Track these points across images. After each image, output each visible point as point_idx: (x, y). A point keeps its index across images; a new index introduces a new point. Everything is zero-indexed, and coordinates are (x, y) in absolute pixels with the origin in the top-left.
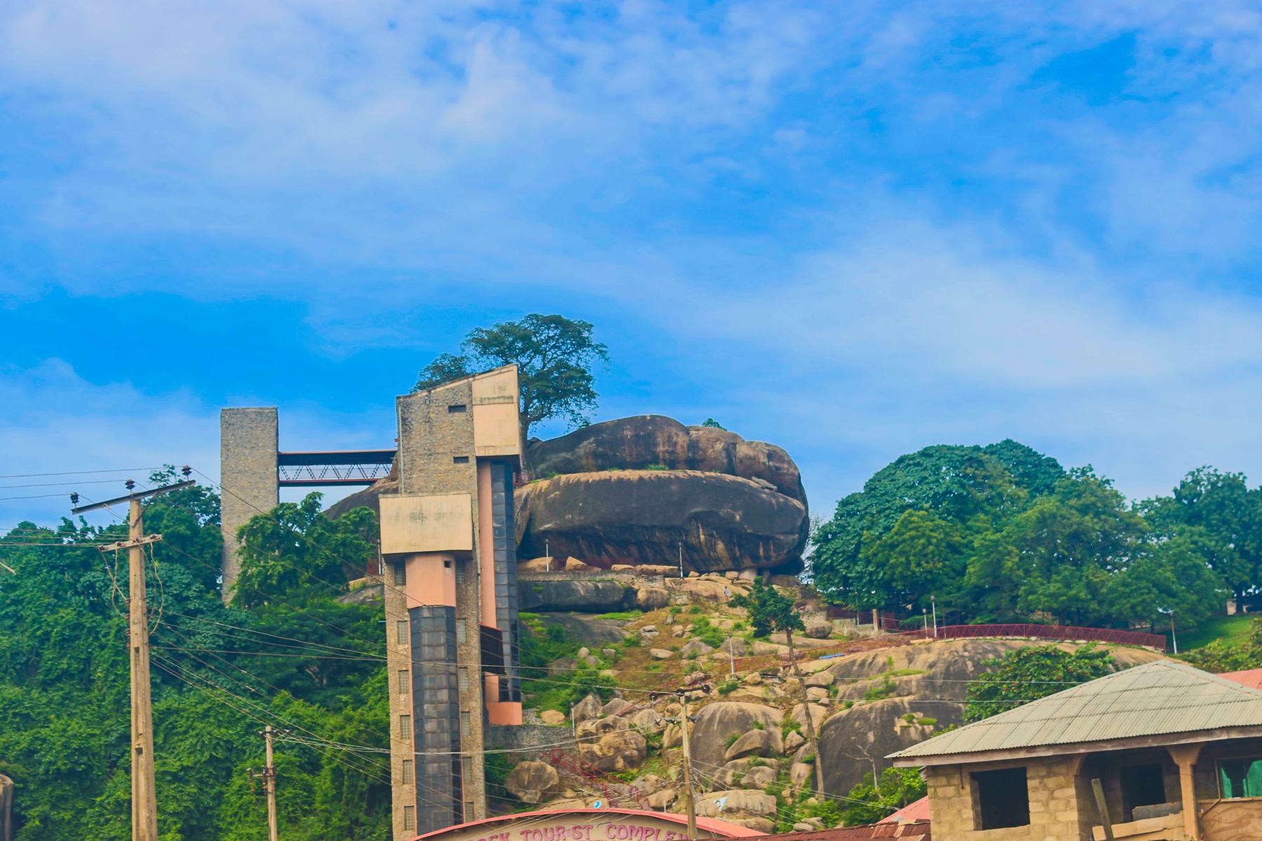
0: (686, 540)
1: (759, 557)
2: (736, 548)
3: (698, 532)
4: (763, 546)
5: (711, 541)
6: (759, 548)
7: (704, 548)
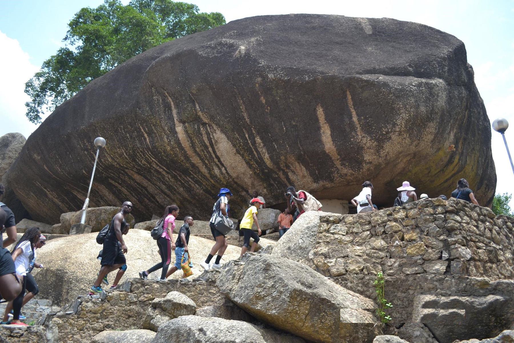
0: (154, 147)
1: (326, 157)
2: (258, 140)
3: (171, 118)
4: (329, 120)
5: (199, 133)
6: (319, 128)
7: (196, 160)
